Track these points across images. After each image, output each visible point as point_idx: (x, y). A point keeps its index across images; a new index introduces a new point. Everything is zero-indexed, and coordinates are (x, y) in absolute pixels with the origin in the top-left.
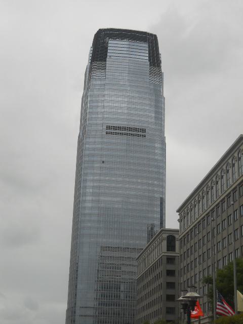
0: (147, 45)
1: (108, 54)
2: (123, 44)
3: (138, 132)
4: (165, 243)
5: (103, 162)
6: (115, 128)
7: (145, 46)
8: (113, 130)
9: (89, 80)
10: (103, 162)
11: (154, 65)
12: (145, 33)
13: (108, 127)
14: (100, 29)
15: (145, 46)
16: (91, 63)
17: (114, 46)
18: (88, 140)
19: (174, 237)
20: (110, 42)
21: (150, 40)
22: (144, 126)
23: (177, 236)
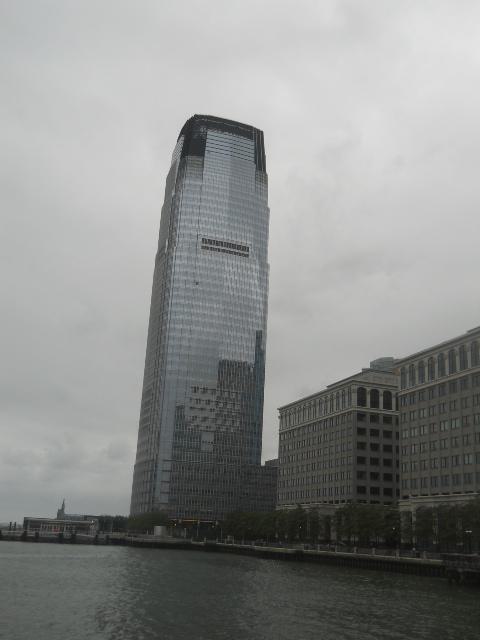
0: (253, 143)
1: (207, 149)
2: (227, 137)
3: (240, 250)
4: (355, 397)
5: (197, 284)
6: (210, 242)
7: (250, 144)
8: (210, 244)
9: (181, 176)
10: (197, 284)
12: (251, 128)
15: (250, 144)
17: (213, 137)
18: (178, 254)
19: (365, 390)
21: (254, 135)
23: (394, 393)
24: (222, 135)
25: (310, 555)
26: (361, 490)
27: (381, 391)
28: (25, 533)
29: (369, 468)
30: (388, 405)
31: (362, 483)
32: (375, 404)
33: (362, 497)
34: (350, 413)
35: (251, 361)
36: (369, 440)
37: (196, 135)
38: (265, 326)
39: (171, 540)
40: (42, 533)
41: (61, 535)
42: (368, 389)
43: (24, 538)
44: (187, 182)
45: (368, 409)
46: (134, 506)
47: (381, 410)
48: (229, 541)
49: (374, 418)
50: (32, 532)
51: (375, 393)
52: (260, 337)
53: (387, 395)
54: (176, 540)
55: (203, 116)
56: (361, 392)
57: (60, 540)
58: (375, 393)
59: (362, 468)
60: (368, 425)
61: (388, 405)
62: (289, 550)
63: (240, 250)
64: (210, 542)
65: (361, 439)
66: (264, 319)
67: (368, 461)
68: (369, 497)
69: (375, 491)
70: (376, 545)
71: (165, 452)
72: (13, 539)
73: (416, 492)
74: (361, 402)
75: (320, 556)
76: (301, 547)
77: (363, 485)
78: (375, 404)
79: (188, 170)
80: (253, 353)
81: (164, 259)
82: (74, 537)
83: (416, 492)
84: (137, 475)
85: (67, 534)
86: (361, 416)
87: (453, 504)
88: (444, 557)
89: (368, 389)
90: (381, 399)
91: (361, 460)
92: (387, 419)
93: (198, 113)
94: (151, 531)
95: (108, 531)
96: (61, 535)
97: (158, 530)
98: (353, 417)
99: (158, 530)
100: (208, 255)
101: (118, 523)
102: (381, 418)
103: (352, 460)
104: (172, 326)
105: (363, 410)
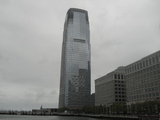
0: (85, 14)
2: (78, 13)
3: (83, 41)
4: (114, 76)
6: (76, 40)
7: (84, 15)
8: (75, 40)
11: (87, 21)
13: (74, 39)
14: (71, 9)
15: (84, 15)
16: (68, 19)
17: (75, 14)
19: (116, 75)
20: (74, 12)
21: (85, 12)
22: (84, 39)
23: (124, 75)
24: (77, 13)
25: (104, 117)
26: (117, 100)
27: (120, 75)
28: (33, 113)
29: (118, 94)
30: (122, 78)
31: (117, 98)
32: (119, 78)
33: (117, 102)
34: (113, 81)
35: (87, 69)
36: (118, 87)
37: (71, 14)
38: (90, 60)
39: (69, 114)
40: (37, 113)
41: (42, 114)
42: (117, 74)
43: (33, 115)
44: (69, 25)
45: (117, 79)
46: (59, 106)
47: (121, 80)
48: (84, 114)
49: (119, 82)
50: (34, 113)
51: (119, 75)
52: (89, 63)
53: (122, 76)
54: (70, 114)
55: (72, 8)
56: (115, 75)
57: (41, 115)
58: (119, 75)
59: (117, 94)
60: (118, 83)
61: (122, 78)
62: (99, 116)
63: (83, 41)
64: (79, 114)
65: (116, 87)
66: (90, 58)
67: (118, 93)
68: (119, 102)
69: (120, 100)
70: (121, 114)
71: (67, 92)
72: (30, 115)
73: (131, 100)
74: (116, 78)
75: (107, 117)
76: (102, 115)
77: (117, 99)
78: (119, 78)
79: (70, 22)
80: (87, 66)
81: (64, 44)
82: (45, 114)
83: (131, 100)
84: (60, 98)
85: (43, 113)
86: (116, 81)
87: (140, 103)
88: (139, 116)
89: (117, 74)
90: (121, 77)
91: (116, 92)
92: (122, 82)
93: (71, 8)
94: (64, 111)
95: (53, 112)
96: (42, 114)
97: (66, 111)
98: (114, 82)
99: (66, 111)
100: (76, 43)
101: (55, 110)
102: (121, 82)
103: (114, 92)
104: (67, 61)
105: (116, 80)
